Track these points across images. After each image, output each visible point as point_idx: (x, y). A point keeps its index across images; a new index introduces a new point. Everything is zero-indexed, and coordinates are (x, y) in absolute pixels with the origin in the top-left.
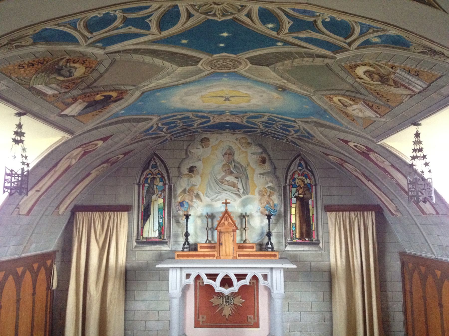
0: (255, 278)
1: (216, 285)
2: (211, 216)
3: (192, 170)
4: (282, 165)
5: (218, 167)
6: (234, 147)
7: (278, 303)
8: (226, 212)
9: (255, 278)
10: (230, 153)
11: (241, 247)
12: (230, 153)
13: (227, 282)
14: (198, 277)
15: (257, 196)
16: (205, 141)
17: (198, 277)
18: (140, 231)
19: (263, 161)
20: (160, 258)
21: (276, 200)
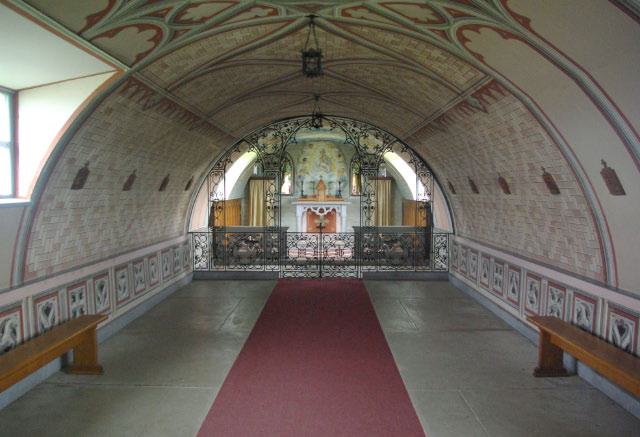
0: (334, 210)
1: (317, 212)
2: (313, 182)
3: (305, 160)
4: (349, 158)
5: (317, 159)
6: (326, 149)
7: (344, 220)
8: (321, 181)
9: (334, 210)
10: (323, 152)
11: (328, 197)
12: (323, 152)
13: (322, 211)
14: (309, 210)
15: (336, 173)
16: (311, 146)
17: (309, 210)
18: (280, 189)
19: (340, 156)
20: (290, 202)
21: (346, 175)
